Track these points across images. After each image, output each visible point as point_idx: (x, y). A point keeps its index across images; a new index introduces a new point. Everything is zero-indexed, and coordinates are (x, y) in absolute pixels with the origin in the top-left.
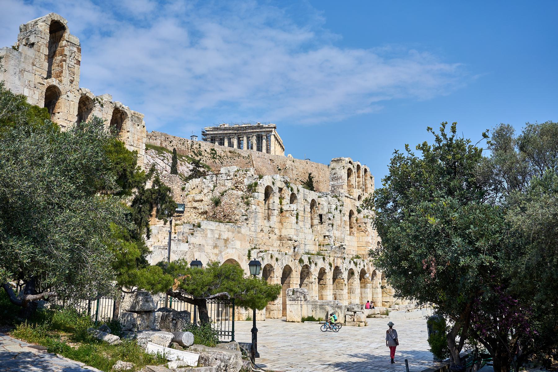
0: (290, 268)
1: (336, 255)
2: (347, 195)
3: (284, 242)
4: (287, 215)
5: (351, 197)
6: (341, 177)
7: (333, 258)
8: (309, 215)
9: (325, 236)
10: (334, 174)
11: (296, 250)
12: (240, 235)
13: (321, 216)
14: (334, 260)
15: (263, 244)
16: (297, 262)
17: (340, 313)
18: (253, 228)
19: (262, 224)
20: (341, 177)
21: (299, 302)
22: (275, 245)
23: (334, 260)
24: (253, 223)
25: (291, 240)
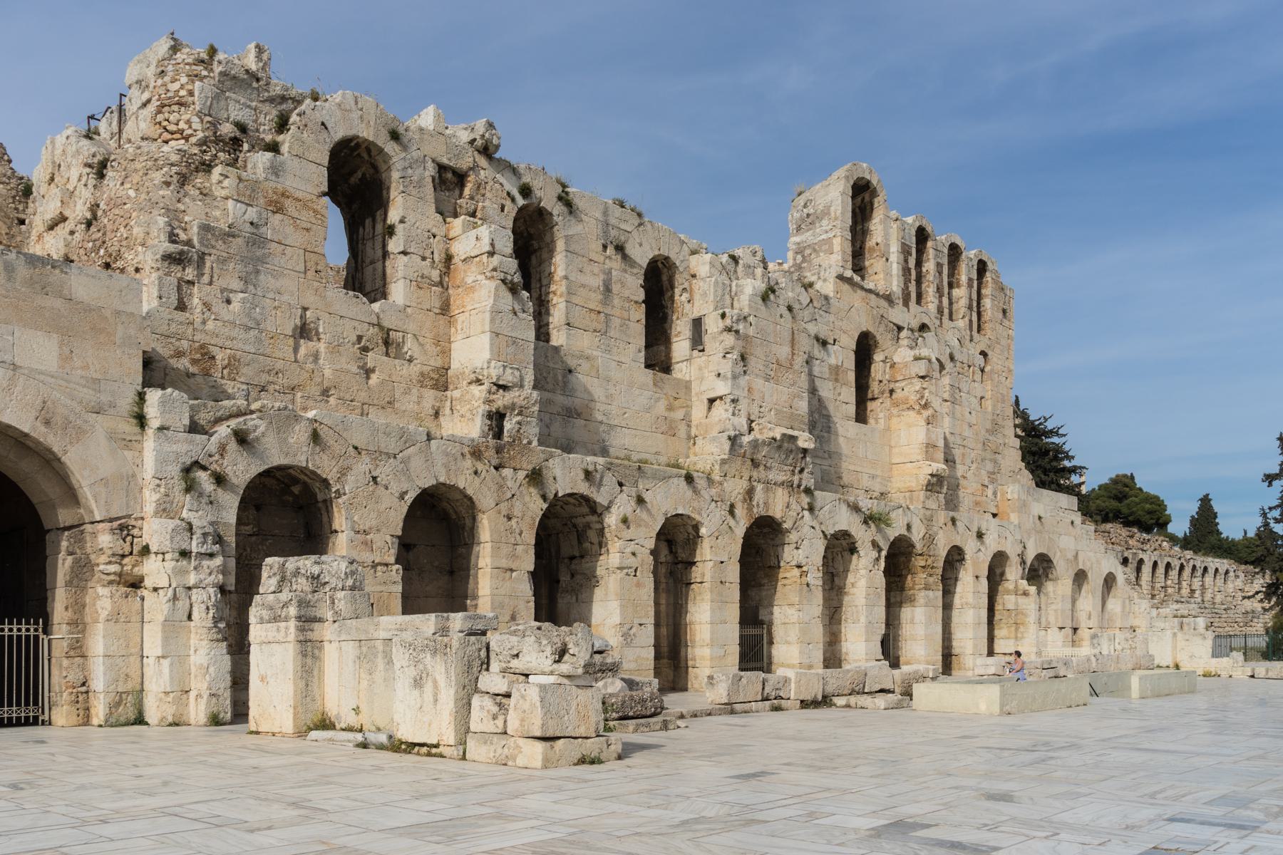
0: (470, 499)
1: (760, 473)
2: (849, 273)
3: (456, 394)
4: (469, 280)
5: (871, 286)
6: (826, 212)
7: (744, 484)
8: (640, 314)
9: (712, 401)
10: (805, 206)
11: (508, 425)
12: (58, 303)
13: (697, 323)
14: (750, 492)
15: (315, 391)
16: (513, 478)
17: (442, 682)
18: (236, 306)
19: (310, 299)
20: (826, 212)
21: (292, 624)
22: (407, 404)
23: (750, 492)
24: (236, 284)
25: (478, 382)
